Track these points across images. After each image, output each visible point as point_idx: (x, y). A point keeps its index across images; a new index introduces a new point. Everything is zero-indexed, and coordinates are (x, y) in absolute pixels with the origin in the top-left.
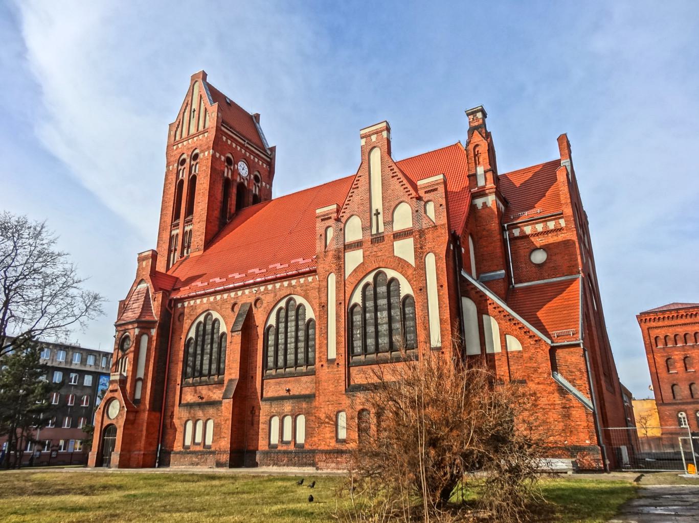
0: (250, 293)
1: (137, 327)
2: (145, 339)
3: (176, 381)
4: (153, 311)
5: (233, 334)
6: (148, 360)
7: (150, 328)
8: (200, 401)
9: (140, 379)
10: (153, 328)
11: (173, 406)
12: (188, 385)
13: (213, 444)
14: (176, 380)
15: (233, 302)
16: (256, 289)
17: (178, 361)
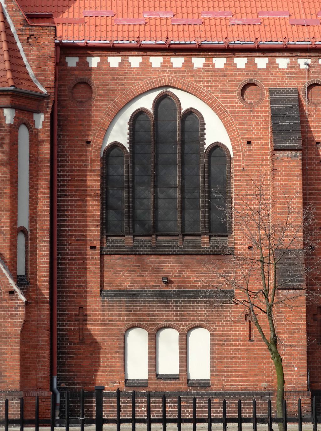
0: (290, 66)
1: (11, 107)
2: (24, 134)
3: (83, 238)
4: (29, 69)
5: (279, 155)
6: (33, 188)
7: (32, 112)
8: (163, 287)
9: (23, 230)
10: (38, 112)
11: (83, 292)
12: (119, 252)
13: (215, 378)
14: (84, 236)
15: (244, 80)
16: (309, 61)
17: (87, 195)
